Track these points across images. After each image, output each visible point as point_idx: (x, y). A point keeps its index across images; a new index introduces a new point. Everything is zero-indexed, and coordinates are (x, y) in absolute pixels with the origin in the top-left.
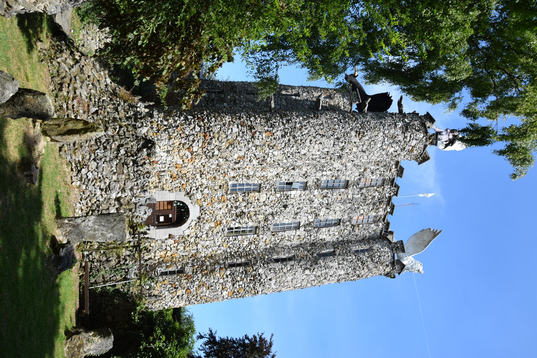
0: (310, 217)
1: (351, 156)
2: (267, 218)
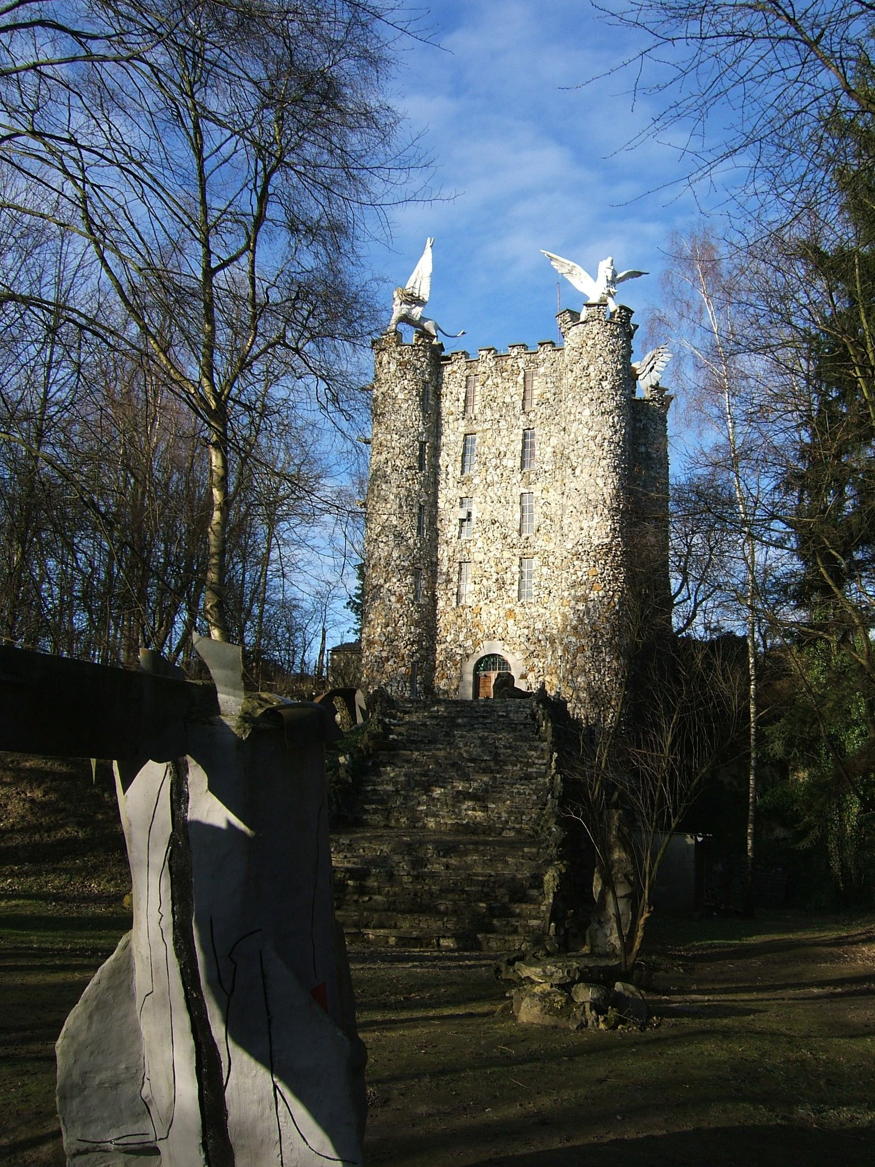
0: (514, 481)
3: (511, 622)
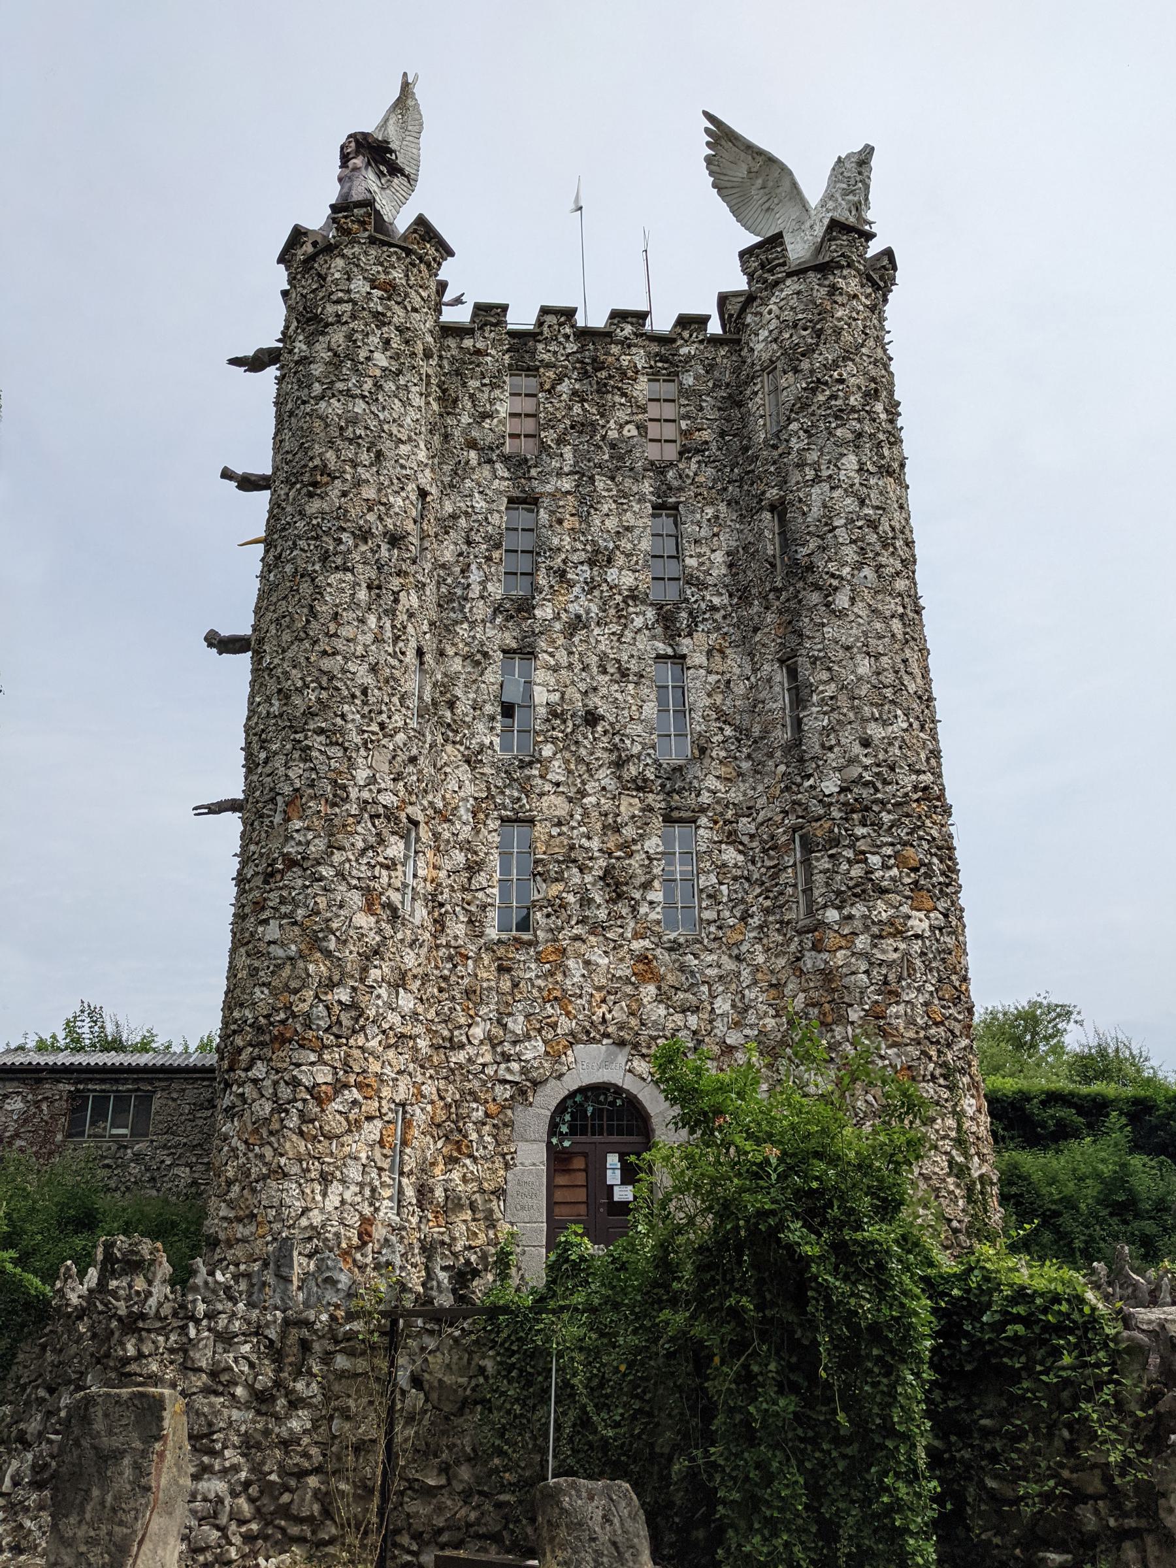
1: (398, 502)
2: (634, 781)
3: (649, 991)
